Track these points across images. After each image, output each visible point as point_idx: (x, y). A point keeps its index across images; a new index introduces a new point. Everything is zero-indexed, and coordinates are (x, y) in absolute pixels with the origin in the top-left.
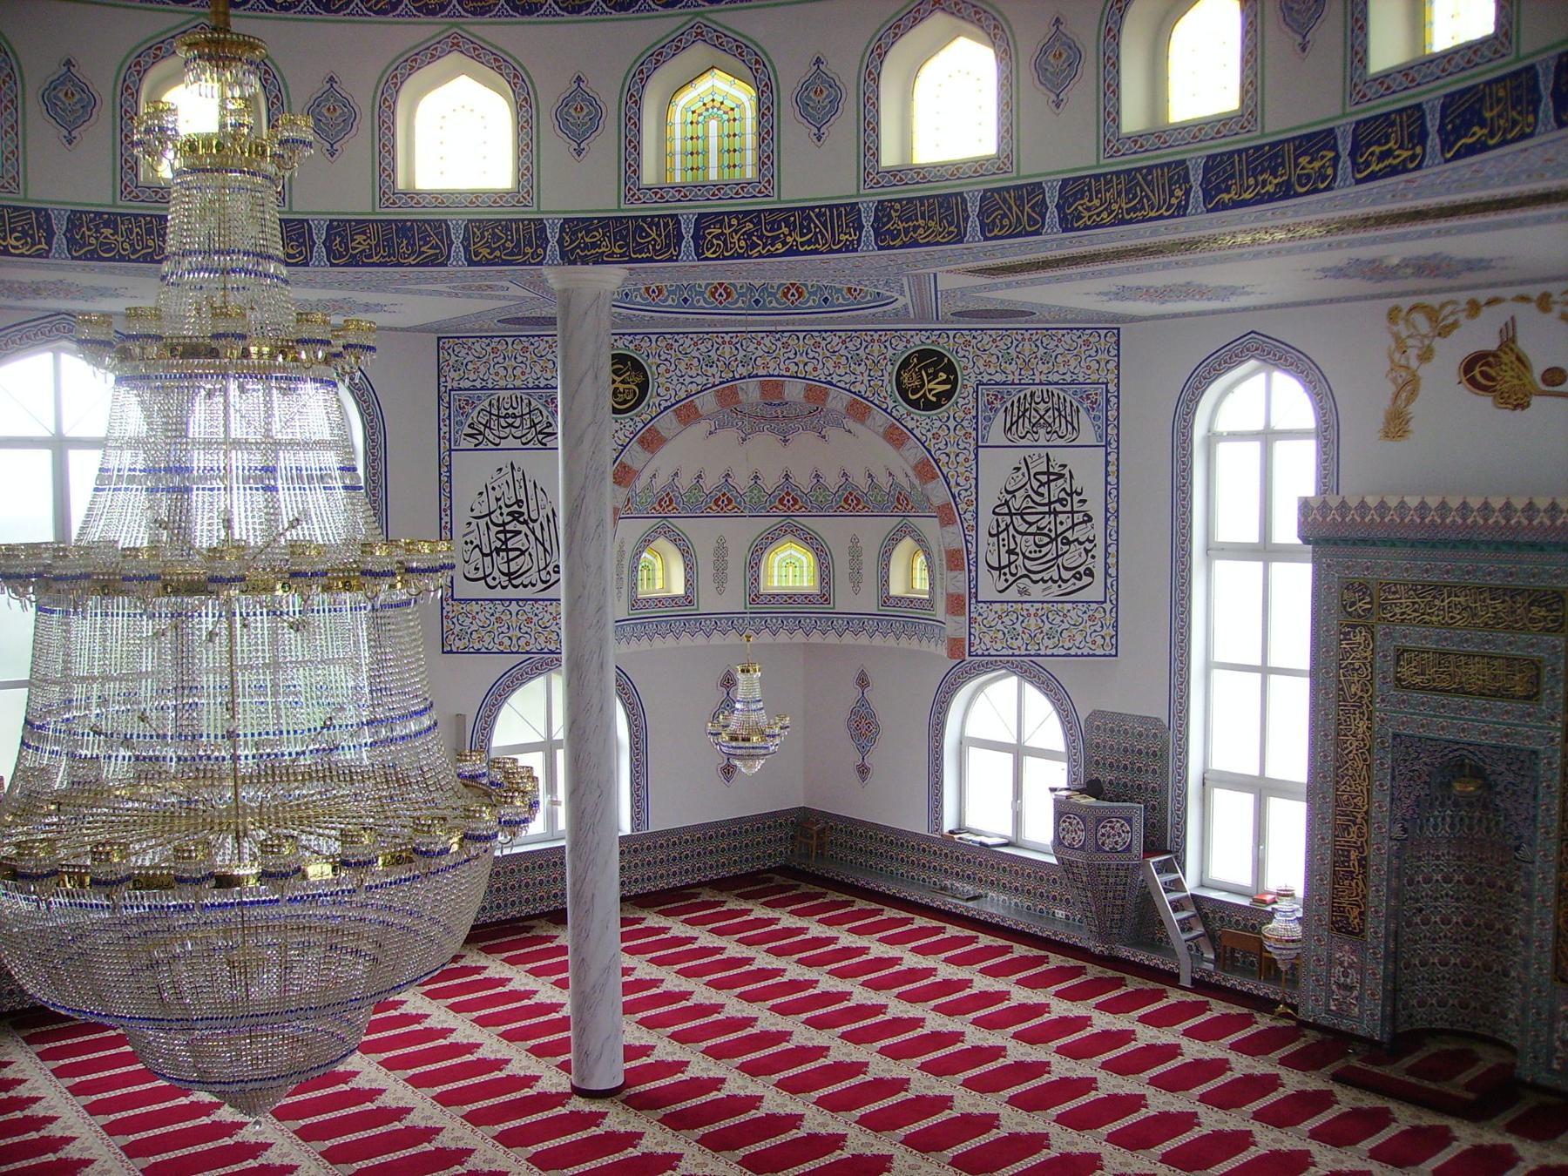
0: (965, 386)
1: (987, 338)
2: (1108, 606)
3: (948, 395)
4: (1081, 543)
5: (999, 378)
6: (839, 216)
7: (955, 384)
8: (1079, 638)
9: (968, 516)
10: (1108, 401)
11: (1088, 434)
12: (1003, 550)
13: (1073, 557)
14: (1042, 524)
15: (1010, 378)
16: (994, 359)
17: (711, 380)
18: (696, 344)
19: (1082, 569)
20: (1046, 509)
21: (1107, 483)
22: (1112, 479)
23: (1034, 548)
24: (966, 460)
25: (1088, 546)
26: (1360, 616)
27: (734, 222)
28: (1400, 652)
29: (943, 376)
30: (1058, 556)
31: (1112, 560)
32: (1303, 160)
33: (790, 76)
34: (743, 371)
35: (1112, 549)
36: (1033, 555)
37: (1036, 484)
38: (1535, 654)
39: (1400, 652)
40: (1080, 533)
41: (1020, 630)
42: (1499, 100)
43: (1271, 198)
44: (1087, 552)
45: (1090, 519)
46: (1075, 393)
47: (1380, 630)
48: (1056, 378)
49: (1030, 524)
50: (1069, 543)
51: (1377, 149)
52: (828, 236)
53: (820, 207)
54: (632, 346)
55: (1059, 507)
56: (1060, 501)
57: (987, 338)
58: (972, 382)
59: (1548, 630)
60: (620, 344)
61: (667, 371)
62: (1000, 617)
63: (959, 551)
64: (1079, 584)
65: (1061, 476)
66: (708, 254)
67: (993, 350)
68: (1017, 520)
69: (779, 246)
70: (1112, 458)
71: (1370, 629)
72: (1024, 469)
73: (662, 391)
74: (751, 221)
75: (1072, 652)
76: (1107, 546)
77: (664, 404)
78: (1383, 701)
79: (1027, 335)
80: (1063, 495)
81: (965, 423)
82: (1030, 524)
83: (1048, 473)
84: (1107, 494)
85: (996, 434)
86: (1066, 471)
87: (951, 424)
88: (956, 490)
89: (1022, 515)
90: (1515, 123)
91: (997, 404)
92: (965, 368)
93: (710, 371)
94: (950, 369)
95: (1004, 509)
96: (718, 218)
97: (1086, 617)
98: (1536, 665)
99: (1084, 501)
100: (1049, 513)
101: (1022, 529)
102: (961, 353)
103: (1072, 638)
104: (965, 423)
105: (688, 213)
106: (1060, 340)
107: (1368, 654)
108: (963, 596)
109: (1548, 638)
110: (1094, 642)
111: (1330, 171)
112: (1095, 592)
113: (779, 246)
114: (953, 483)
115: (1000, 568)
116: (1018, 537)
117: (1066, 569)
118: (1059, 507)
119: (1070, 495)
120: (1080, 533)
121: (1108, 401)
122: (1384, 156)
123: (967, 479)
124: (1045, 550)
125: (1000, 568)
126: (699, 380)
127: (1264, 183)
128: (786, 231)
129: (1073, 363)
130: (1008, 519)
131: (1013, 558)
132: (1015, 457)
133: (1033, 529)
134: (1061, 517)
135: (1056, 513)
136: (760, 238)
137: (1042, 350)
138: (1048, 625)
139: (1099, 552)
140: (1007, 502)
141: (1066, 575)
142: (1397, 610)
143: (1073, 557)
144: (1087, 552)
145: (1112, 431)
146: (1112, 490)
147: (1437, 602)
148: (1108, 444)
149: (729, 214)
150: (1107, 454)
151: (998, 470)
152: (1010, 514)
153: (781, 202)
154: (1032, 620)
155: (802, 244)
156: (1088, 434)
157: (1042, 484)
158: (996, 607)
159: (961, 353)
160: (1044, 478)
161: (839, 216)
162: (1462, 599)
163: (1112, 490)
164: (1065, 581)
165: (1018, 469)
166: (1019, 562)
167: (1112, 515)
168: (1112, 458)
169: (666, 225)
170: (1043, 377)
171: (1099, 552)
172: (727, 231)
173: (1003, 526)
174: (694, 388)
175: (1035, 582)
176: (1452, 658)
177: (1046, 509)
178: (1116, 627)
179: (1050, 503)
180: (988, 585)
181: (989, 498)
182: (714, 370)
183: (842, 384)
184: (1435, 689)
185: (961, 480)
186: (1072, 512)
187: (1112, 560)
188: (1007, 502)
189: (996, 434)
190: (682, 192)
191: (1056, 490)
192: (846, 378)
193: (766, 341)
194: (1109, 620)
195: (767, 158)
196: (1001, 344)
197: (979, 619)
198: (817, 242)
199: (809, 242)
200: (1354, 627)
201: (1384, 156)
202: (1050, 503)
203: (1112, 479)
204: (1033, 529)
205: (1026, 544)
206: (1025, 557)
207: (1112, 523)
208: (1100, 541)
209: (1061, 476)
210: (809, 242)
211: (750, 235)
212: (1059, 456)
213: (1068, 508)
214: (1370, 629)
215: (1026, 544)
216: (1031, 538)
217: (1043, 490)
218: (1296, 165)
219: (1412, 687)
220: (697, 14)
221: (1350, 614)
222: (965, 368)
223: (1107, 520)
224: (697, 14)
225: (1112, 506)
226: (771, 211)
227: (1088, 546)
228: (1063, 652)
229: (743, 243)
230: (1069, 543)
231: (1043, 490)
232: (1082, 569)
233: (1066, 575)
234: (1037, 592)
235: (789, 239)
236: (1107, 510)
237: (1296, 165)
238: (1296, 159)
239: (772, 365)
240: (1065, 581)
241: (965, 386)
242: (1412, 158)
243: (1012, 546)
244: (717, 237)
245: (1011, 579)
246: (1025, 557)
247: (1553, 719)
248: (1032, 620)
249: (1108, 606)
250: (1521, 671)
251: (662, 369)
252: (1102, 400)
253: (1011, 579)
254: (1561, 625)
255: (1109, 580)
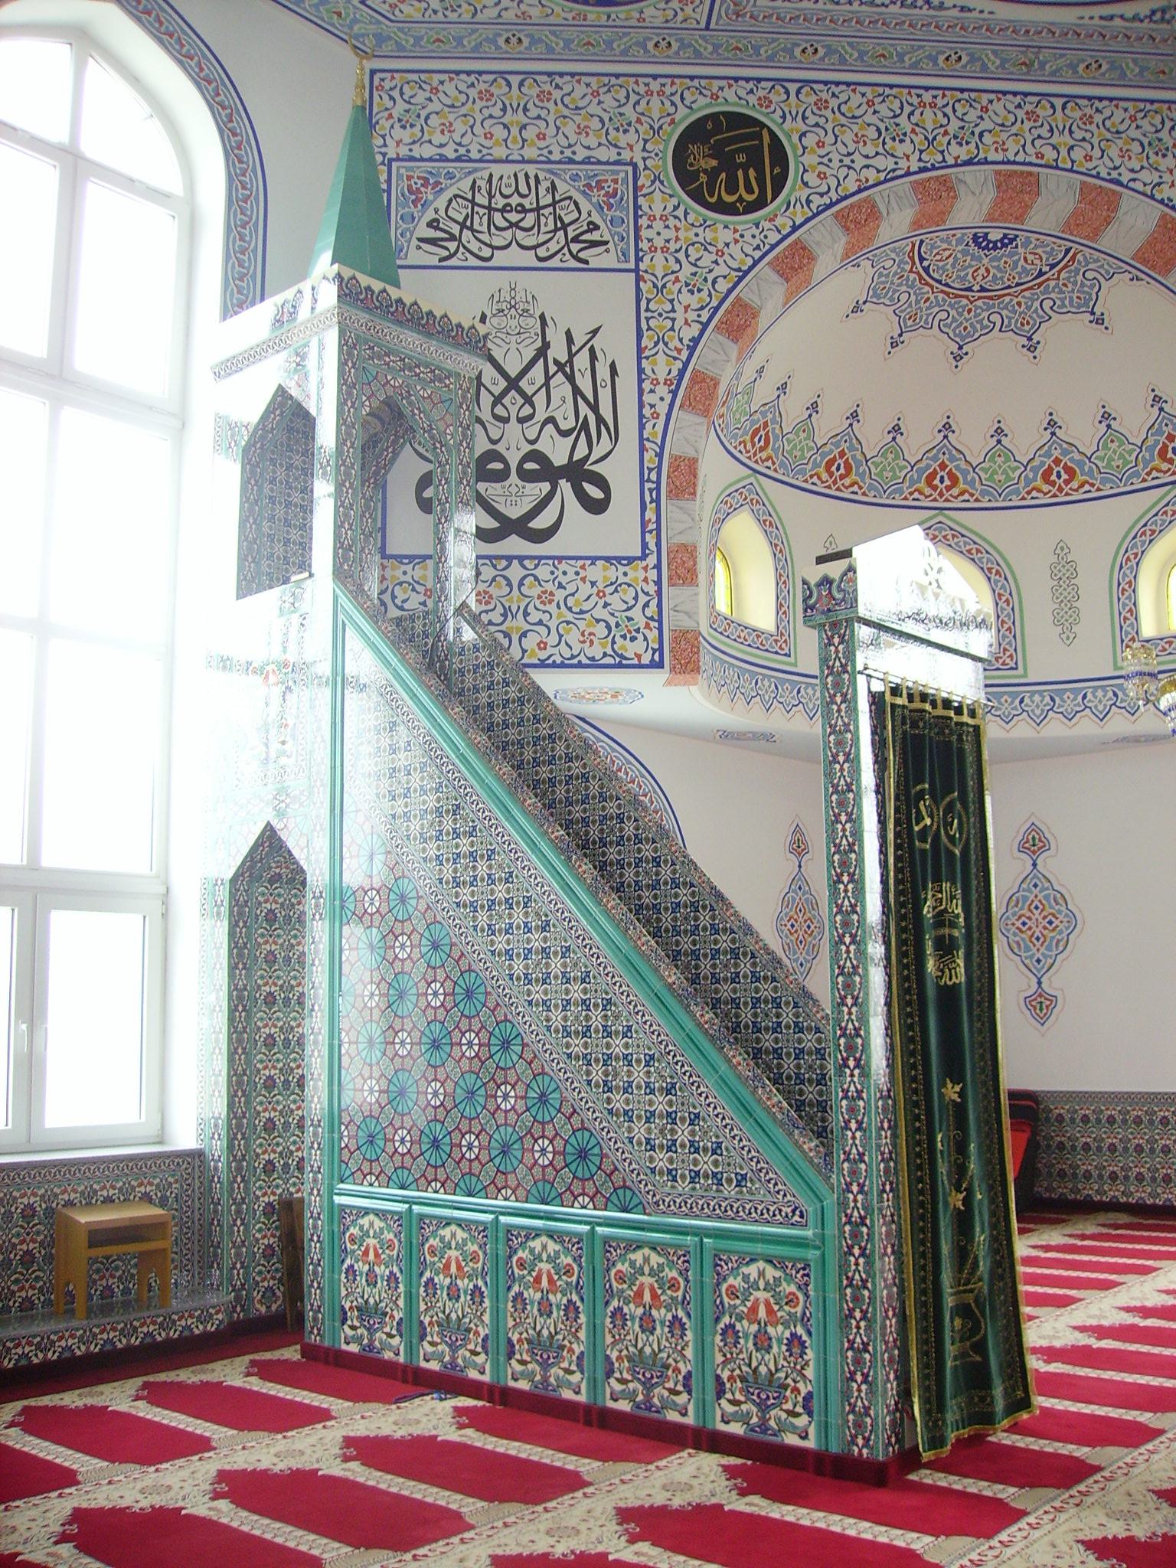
17: (903, 164)
18: (870, 103)
34: (963, 153)
54: (753, 100)
60: (729, 94)
61: (820, 144)
73: (811, 178)
77: (817, 201)
93: (901, 149)
126: (881, 162)
174: (872, 176)
182: (907, 147)
183: (1138, 186)
192: (1145, 176)
193: (997, 106)
239: (1012, 146)
251: (810, 141)
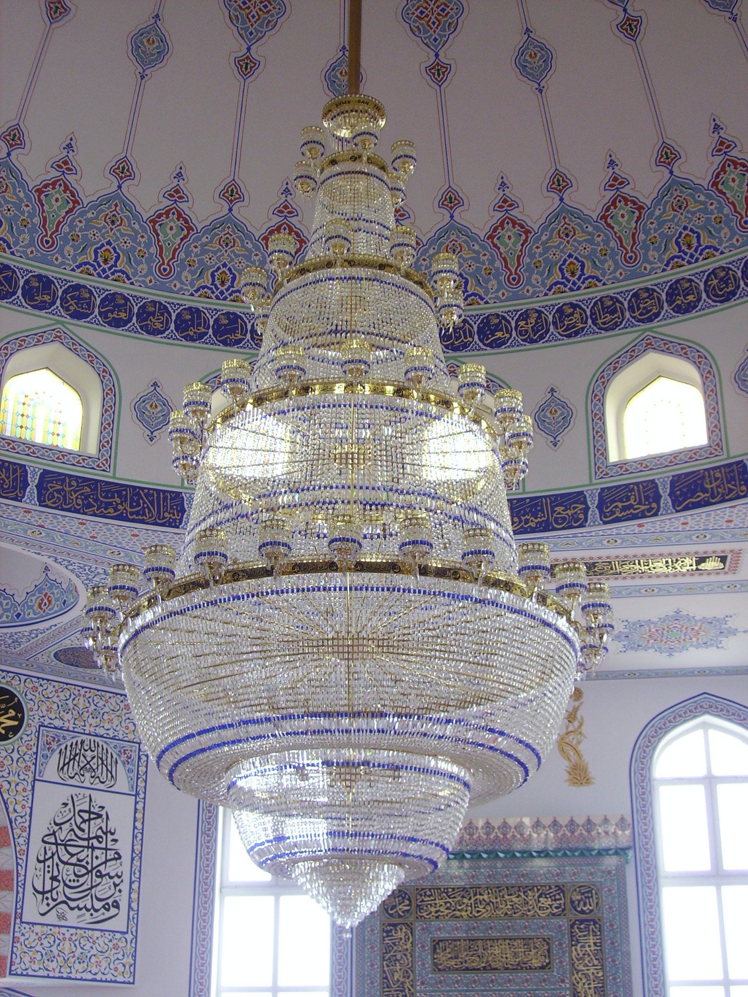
0: (29, 725)
1: (51, 688)
2: (129, 937)
3: (15, 730)
4: (111, 878)
5: (58, 723)
6: (165, 499)
7: (21, 721)
8: (104, 964)
9: (21, 841)
10: (139, 758)
11: (123, 783)
12: (48, 876)
13: (104, 889)
14: (82, 856)
15: (67, 724)
16: (55, 707)
19: (110, 901)
20: (85, 843)
21: (135, 827)
22: (139, 825)
23: (73, 877)
24: (24, 790)
25: (117, 880)
26: (400, 916)
27: (74, 483)
28: (436, 944)
29: (12, 713)
30: (92, 887)
31: (134, 896)
32: (559, 509)
33: (132, 389)
35: (135, 886)
36: (72, 884)
37: (79, 820)
38: (546, 933)
39: (436, 944)
40: (111, 868)
41: (56, 952)
42: (716, 479)
43: (533, 530)
44: (116, 885)
45: (120, 857)
46: (115, 747)
47: (418, 926)
48: (101, 731)
49: (72, 855)
50: (101, 876)
51: (620, 505)
52: (155, 513)
53: (149, 489)
55: (96, 843)
56: (97, 837)
57: (51, 688)
58: (36, 723)
59: (553, 914)
62: (40, 939)
63: (10, 873)
64: (108, 914)
65: (99, 816)
66: (49, 503)
67: (55, 699)
68: (61, 850)
69: (111, 510)
70: (140, 806)
71: (410, 927)
72: (70, 806)
74: (88, 486)
75: (98, 977)
76: (131, 883)
78: (422, 983)
79: (83, 691)
80: (100, 833)
81: (27, 757)
82: (72, 855)
83: (90, 812)
84: (134, 837)
85: (51, 771)
86: (103, 813)
87: (15, 756)
88: (13, 816)
89: (65, 845)
90: (730, 491)
91: (54, 745)
92: (31, 710)
94: (19, 708)
95: (51, 839)
96: (61, 478)
97: (111, 945)
98: (547, 941)
99: (115, 841)
100: (88, 847)
101: (66, 858)
102: (29, 696)
103: (98, 964)
104: (27, 757)
105: (35, 468)
106: (107, 701)
107: (409, 945)
108: (10, 916)
109: (555, 921)
110: (116, 969)
111: (582, 516)
112: (119, 923)
113: (111, 510)
114: (11, 809)
115: (43, 893)
116: (61, 865)
117: (99, 900)
118: (96, 843)
119: (106, 834)
120: (111, 868)
121: (139, 758)
122: (624, 509)
123: (23, 807)
124: (82, 880)
125: (43, 893)
127: (527, 522)
128: (118, 500)
129: (116, 722)
130: (54, 847)
131: (55, 884)
132: (64, 793)
133: (74, 860)
134: (97, 852)
135: (93, 848)
136: (96, 500)
137: (93, 707)
138: (80, 950)
139: (125, 887)
140: (54, 833)
141: (98, 905)
142: (433, 909)
143: (104, 889)
144: (116, 885)
145: (141, 784)
146: (138, 834)
147: (465, 900)
148: (137, 794)
149: (70, 476)
150: (136, 803)
151: (49, 803)
152: (56, 844)
153: (114, 477)
154: (67, 943)
155: (132, 514)
156: (123, 783)
157: (84, 821)
158: (37, 928)
159: (29, 696)
160: (86, 816)
161: (165, 499)
162: (486, 897)
163: (138, 834)
164: (96, 911)
165: (66, 804)
166: (60, 889)
167: (137, 855)
168: (140, 806)
169: (15, 471)
170: (92, 729)
171: (125, 887)
172: (67, 489)
173: (49, 854)
175: (72, 909)
176: (480, 942)
177: (85, 843)
178: (134, 957)
179: (89, 839)
180: (32, 908)
181: (40, 827)
184: (467, 969)
185: (18, 808)
186: (106, 849)
187: (134, 896)
188: (54, 833)
189: (51, 771)
190: (32, 448)
191: (94, 827)
194: (129, 950)
195: (107, 442)
196: (61, 695)
197: (22, 939)
198: (144, 514)
199: (137, 513)
200: (395, 925)
201: (624, 509)
202: (89, 839)
203: (139, 825)
204: (74, 860)
205: (67, 873)
206: (65, 885)
207: (136, 863)
208: (126, 877)
209: (99, 816)
210: (137, 513)
211: (87, 497)
212: (100, 799)
213: (103, 845)
214: (410, 927)
215: (67, 873)
216: (71, 867)
217: (85, 826)
218: (553, 512)
219: (449, 969)
220: (58, 322)
221: (391, 915)
222: (31, 710)
223: (133, 859)
224: (58, 322)
225: (137, 848)
226: (107, 483)
227: (117, 880)
228: (89, 976)
229: (80, 502)
230: (101, 876)
231: (85, 826)
232: (110, 901)
233: (98, 905)
234: (72, 918)
235: (120, 507)
236: (133, 851)
237: (553, 512)
238: (552, 508)
240: (96, 911)
241: (29, 725)
242: (649, 510)
243: (56, 873)
244: (58, 491)
245: (52, 904)
246: (65, 885)
247: (563, 981)
248: (67, 943)
249: (129, 937)
250: (535, 948)
252: (135, 756)
253: (52, 904)
254: (564, 910)
255: (132, 913)
